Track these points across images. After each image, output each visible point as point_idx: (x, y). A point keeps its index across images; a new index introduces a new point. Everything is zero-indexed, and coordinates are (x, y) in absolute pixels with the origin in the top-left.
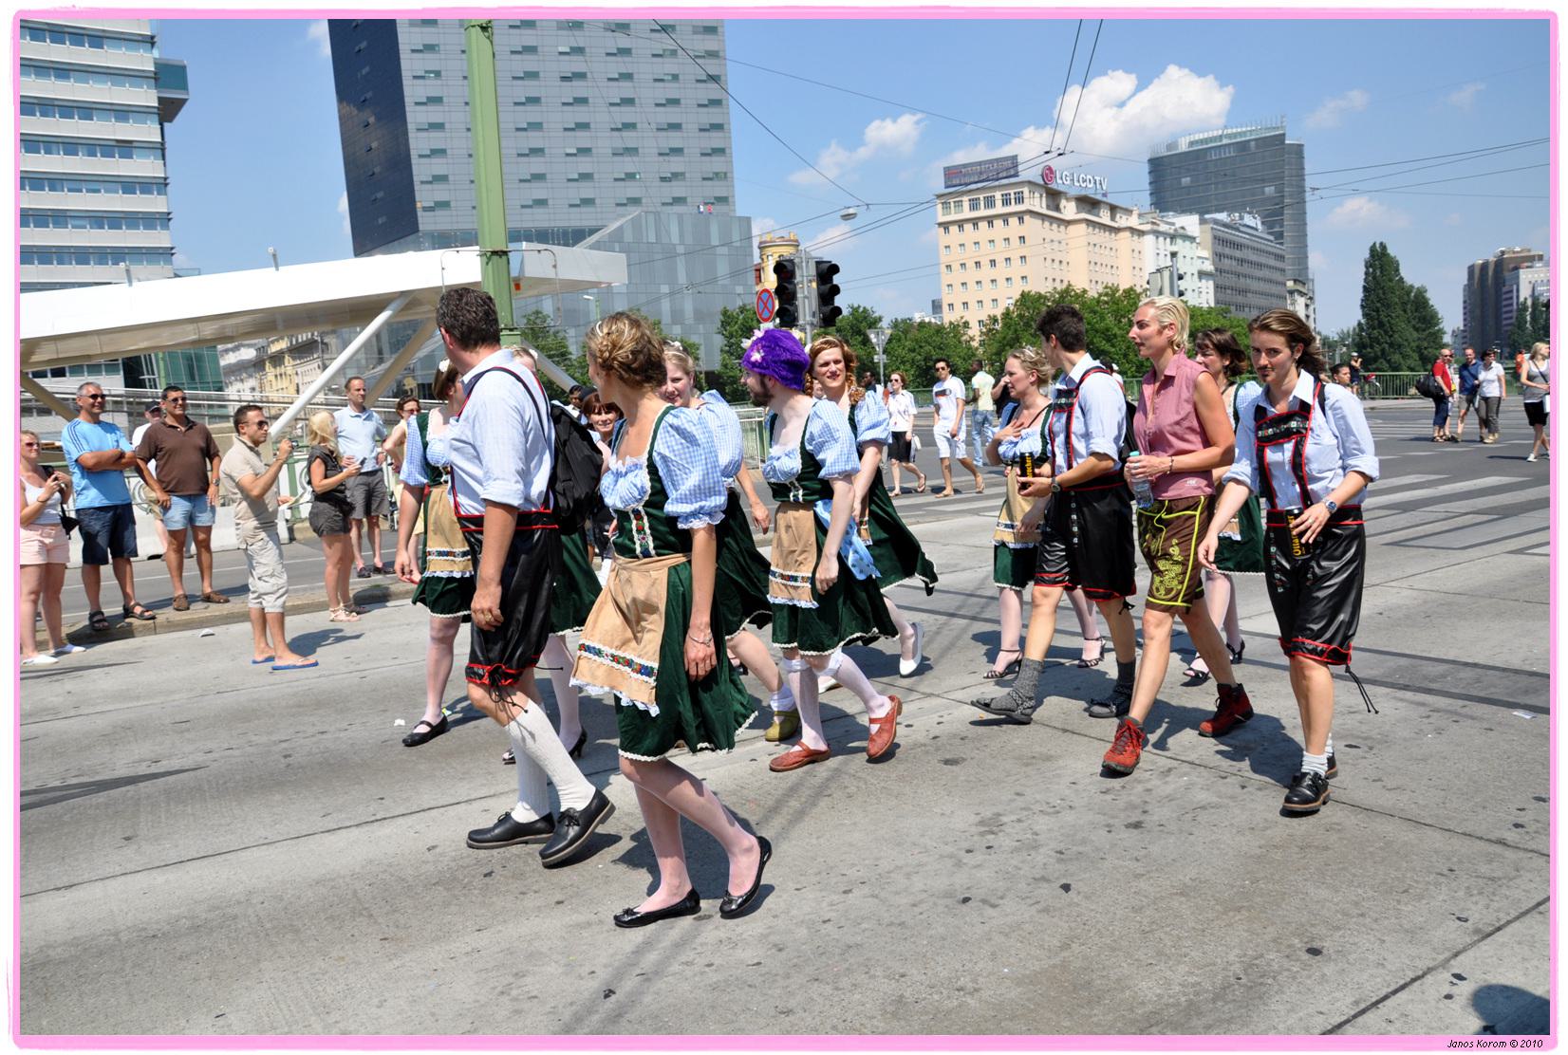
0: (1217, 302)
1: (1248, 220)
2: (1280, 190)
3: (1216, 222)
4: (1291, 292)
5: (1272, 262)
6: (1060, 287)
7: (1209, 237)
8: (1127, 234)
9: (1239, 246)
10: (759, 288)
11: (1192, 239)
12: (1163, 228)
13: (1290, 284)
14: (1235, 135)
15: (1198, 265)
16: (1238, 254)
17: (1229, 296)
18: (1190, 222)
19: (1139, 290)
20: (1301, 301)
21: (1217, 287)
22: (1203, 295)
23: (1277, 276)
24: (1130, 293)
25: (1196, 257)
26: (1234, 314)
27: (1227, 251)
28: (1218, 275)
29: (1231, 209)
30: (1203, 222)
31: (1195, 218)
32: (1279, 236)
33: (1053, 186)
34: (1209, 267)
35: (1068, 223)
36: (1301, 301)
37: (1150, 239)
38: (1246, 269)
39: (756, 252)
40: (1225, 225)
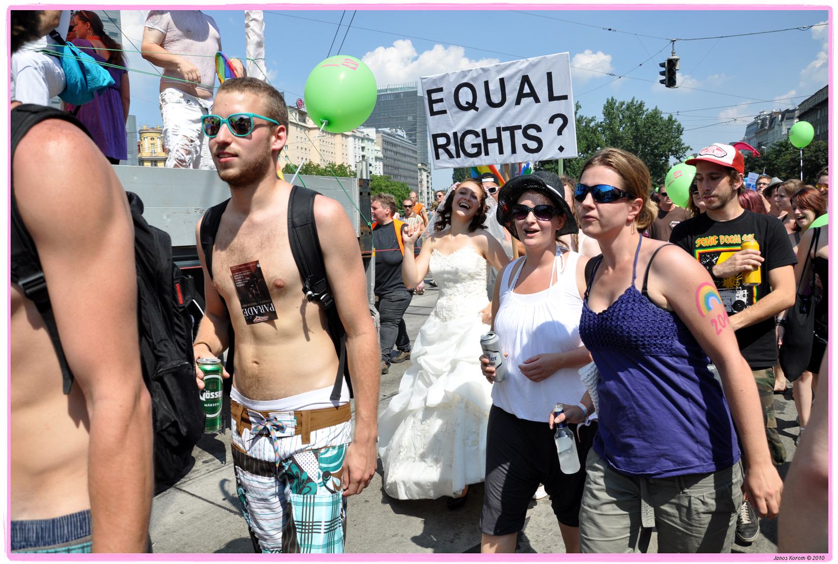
0: (384, 173)
1: (400, 132)
2: (415, 118)
3: (384, 133)
4: (420, 169)
5: (411, 154)
6: (308, 162)
7: (380, 140)
8: (339, 137)
9: (395, 145)
10: (139, 155)
11: (372, 140)
12: (358, 134)
13: (419, 165)
14: (393, 89)
15: (375, 154)
16: (394, 149)
17: (390, 170)
18: (371, 132)
19: (346, 166)
20: (425, 174)
21: (384, 165)
22: (378, 170)
23: (413, 161)
24: (341, 166)
25: (374, 150)
26: (393, 179)
27: (389, 147)
28: (385, 160)
29: (391, 127)
30: (377, 132)
31: (374, 130)
32: (414, 141)
33: (303, 109)
34: (380, 155)
35: (310, 129)
36: (425, 174)
37: (351, 139)
38: (398, 157)
39: (138, 135)
40: (388, 134)
